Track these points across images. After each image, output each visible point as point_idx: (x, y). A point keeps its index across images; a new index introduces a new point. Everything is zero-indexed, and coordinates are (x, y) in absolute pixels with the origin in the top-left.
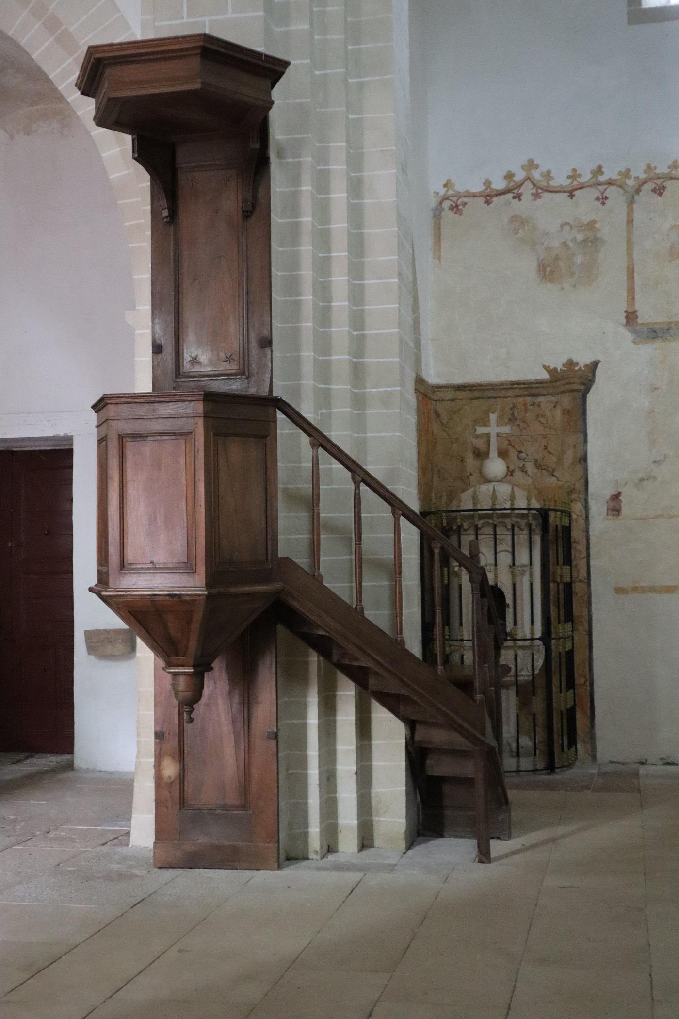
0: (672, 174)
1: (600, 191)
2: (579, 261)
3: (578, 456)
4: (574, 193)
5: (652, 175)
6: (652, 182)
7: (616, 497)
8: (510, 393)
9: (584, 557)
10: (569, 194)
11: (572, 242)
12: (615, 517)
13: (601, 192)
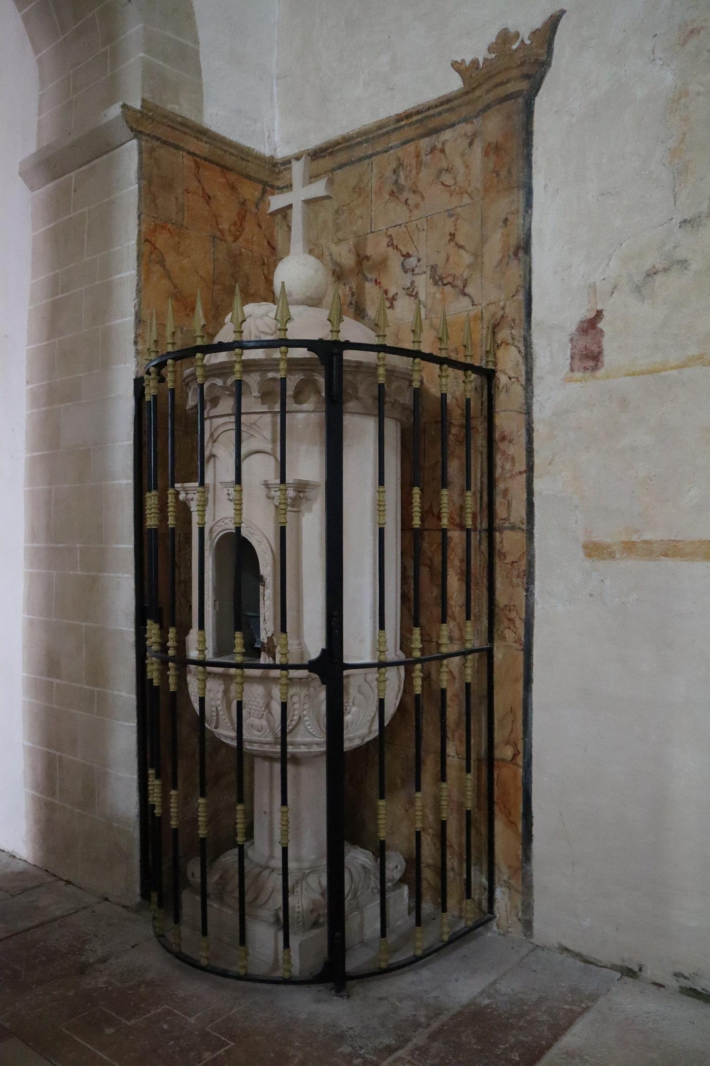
3: (513, 241)
8: (395, 140)
9: (521, 473)
12: (588, 374)
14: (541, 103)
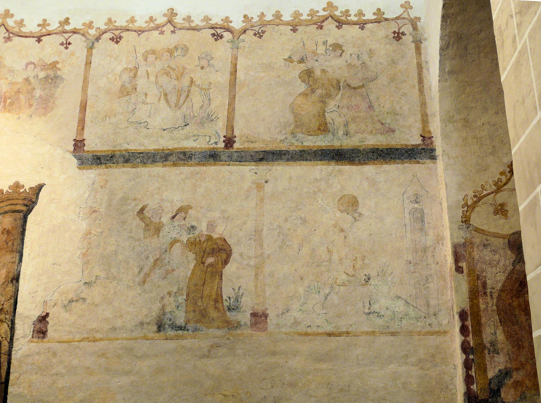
0: (129, 27)
1: (64, 37)
2: (38, 95)
3: (11, 275)
4: (42, 38)
5: (111, 27)
6: (111, 32)
7: (43, 319)
10: (37, 39)
11: (34, 79)
12: (40, 340)
13: (65, 38)
14: (30, 218)
